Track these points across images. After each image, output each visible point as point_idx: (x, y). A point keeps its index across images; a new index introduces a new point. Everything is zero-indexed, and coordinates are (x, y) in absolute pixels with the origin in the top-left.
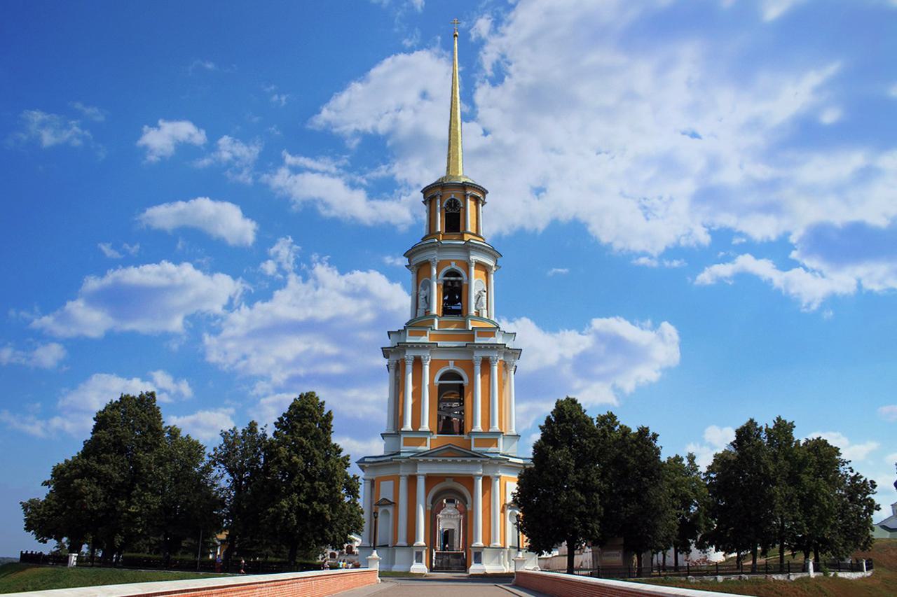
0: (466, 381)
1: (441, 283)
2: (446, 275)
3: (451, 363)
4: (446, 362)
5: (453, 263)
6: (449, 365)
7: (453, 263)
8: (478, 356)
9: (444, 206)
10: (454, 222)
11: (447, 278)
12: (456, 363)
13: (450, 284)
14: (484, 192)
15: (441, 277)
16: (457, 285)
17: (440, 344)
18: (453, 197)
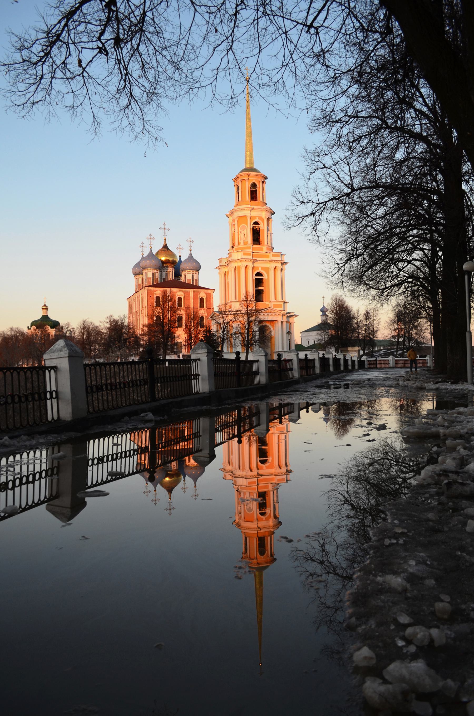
0: (265, 277)
1: (252, 227)
2: (254, 223)
3: (260, 268)
4: (258, 268)
5: (257, 218)
6: (258, 269)
7: (257, 218)
8: (273, 265)
9: (250, 186)
10: (254, 195)
11: (254, 225)
12: (263, 268)
13: (255, 229)
14: (266, 178)
15: (252, 226)
16: (258, 229)
17: (258, 259)
18: (254, 181)
